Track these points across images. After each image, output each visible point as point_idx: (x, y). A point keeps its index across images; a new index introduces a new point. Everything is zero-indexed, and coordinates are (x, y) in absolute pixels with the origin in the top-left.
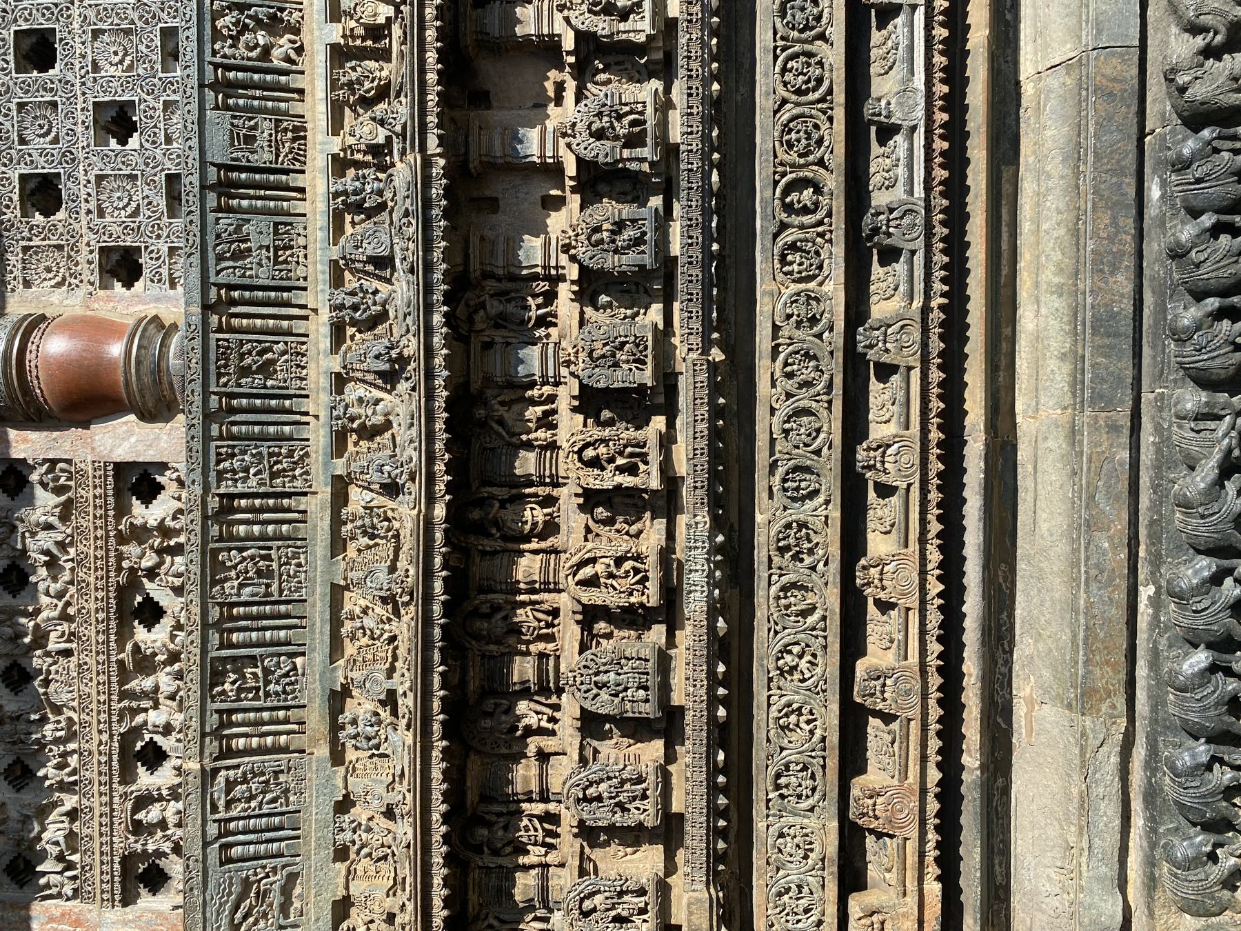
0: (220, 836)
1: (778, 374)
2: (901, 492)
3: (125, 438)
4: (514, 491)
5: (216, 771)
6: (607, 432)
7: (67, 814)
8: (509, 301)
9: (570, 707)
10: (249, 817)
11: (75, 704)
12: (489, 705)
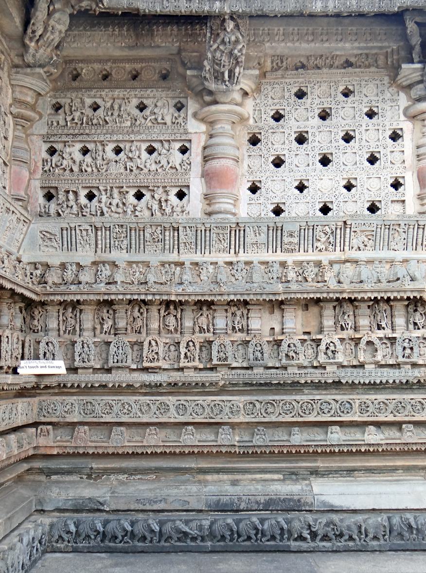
0: (70, 227)
1: (216, 402)
2: (178, 440)
3: (197, 188)
4: (179, 319)
5: (91, 226)
6: (198, 349)
7: (71, 169)
8: (240, 317)
9: (111, 338)
10: (76, 236)
11: (109, 171)
12: (111, 312)
